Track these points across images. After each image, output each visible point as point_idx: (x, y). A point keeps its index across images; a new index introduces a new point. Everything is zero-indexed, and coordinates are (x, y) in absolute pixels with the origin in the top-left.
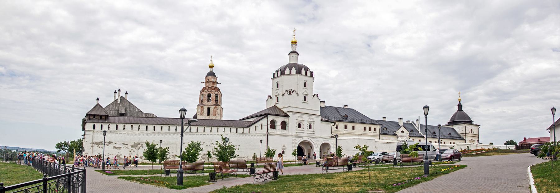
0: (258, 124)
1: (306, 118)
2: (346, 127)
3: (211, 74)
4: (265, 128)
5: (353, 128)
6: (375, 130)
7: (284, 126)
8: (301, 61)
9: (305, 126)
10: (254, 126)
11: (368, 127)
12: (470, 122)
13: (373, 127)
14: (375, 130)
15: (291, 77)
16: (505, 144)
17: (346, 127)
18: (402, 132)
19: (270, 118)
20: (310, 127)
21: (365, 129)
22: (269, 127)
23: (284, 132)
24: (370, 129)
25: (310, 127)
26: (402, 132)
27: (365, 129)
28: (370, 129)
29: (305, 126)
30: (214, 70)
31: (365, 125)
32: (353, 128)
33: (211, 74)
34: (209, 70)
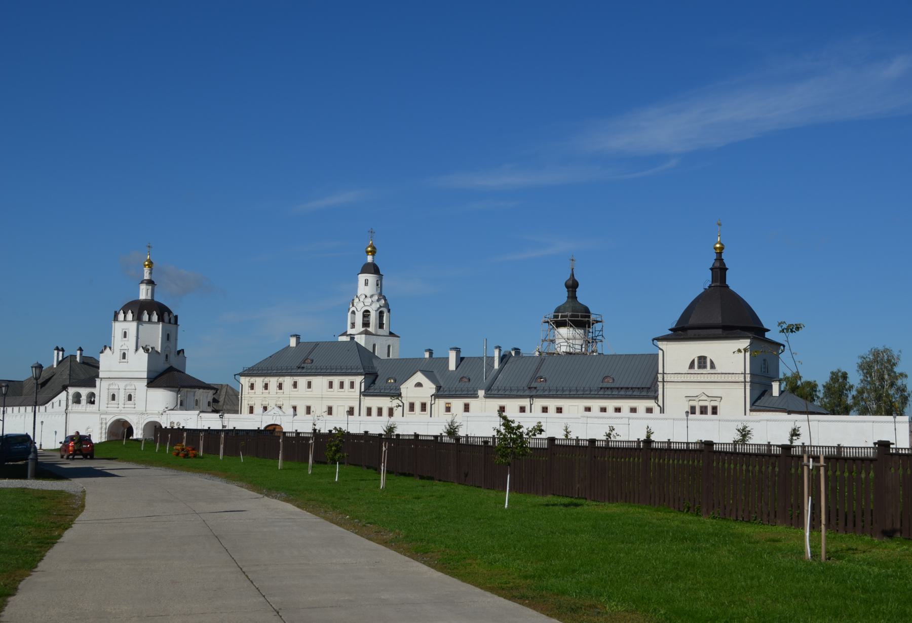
0: (56, 400)
1: (122, 384)
2: (295, 385)
4: (64, 404)
5: (309, 385)
6: (352, 385)
7: (91, 400)
9: (122, 397)
11: (336, 380)
13: (347, 380)
14: (352, 385)
17: (295, 385)
18: (419, 385)
19: (72, 391)
20: (130, 398)
21: (331, 385)
22: (70, 402)
23: (91, 408)
24: (342, 385)
25: (130, 398)
26: (419, 385)
27: (331, 385)
28: (342, 385)
29: (122, 397)
32: (309, 385)
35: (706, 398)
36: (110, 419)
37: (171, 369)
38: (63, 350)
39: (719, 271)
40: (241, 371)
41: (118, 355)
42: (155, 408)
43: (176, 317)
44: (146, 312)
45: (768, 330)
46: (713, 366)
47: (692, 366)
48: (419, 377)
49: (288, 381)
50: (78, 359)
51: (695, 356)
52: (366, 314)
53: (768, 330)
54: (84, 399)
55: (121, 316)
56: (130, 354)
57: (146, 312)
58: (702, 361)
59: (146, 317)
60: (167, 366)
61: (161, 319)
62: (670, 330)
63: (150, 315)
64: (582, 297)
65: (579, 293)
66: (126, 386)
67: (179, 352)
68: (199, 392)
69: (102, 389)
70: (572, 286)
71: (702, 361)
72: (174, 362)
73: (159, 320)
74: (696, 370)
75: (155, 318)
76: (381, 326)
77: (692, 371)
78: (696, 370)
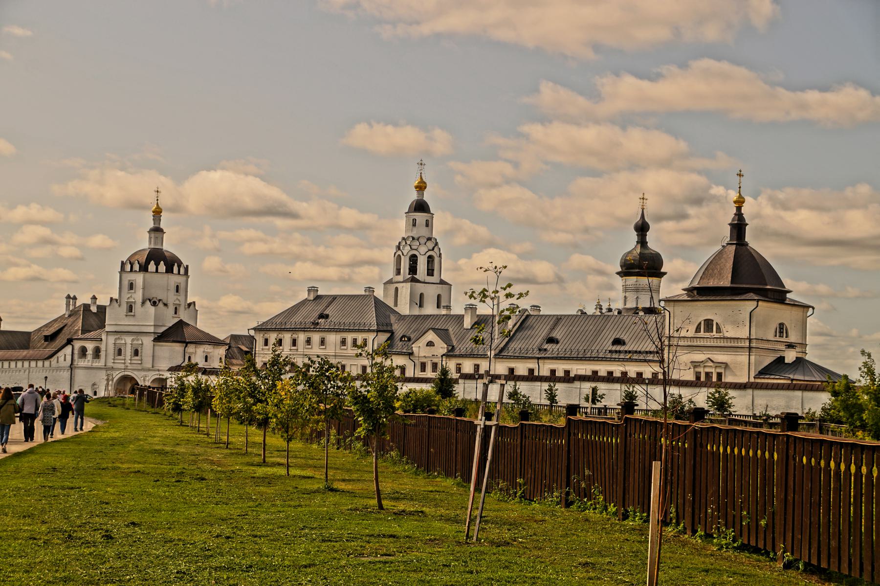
0: (61, 354)
1: (128, 339)
3: (421, 207)
7: (97, 352)
8: (168, 246)
9: (128, 351)
10: (55, 357)
12: (779, 296)
15: (156, 275)
16: (169, 370)
20: (136, 353)
21: (343, 342)
26: (430, 344)
27: (343, 342)
30: (427, 197)
31: (344, 335)
33: (421, 207)
34: (414, 196)
35: (711, 364)
36: (117, 375)
37: (181, 324)
38: (75, 298)
39: (739, 227)
40: (255, 325)
41: (124, 307)
42: (159, 364)
43: (186, 269)
44: (152, 262)
45: (789, 292)
46: (719, 330)
47: (698, 330)
48: (431, 336)
49: (302, 337)
50: (92, 308)
51: (701, 319)
52: (414, 259)
53: (789, 292)
54: (90, 352)
55: (128, 267)
56: (138, 308)
57: (152, 262)
58: (709, 324)
59: (152, 267)
60: (176, 320)
61: (169, 270)
62: (684, 290)
63: (157, 264)
64: (653, 242)
65: (650, 237)
66: (133, 340)
67: (189, 305)
68: (208, 348)
69: (108, 343)
70: (642, 229)
71: (709, 324)
72: (184, 316)
73: (167, 272)
74: (702, 334)
75: (162, 267)
76: (430, 272)
77: (699, 335)
78: (702, 334)
